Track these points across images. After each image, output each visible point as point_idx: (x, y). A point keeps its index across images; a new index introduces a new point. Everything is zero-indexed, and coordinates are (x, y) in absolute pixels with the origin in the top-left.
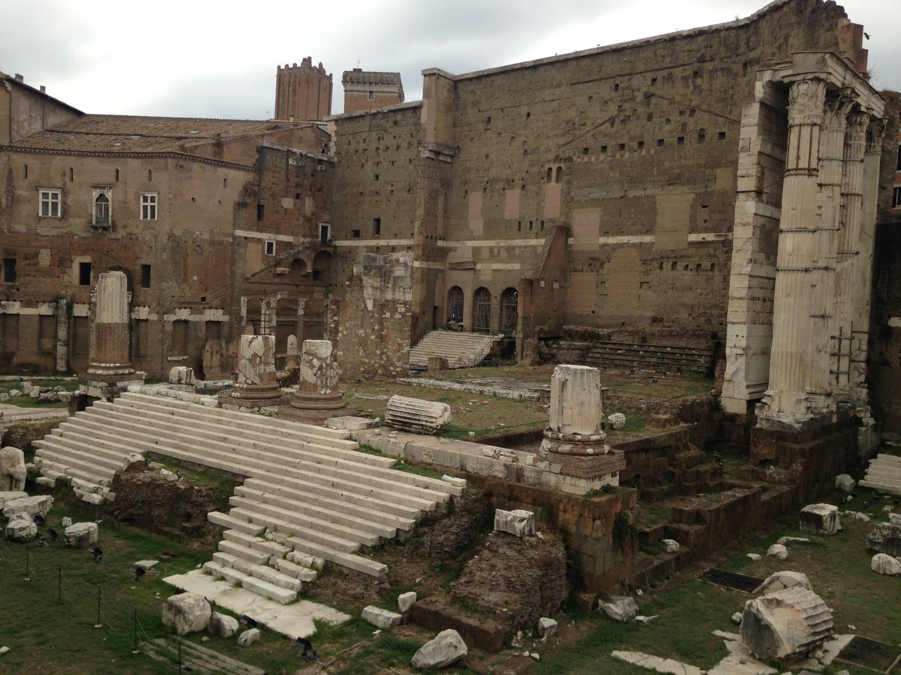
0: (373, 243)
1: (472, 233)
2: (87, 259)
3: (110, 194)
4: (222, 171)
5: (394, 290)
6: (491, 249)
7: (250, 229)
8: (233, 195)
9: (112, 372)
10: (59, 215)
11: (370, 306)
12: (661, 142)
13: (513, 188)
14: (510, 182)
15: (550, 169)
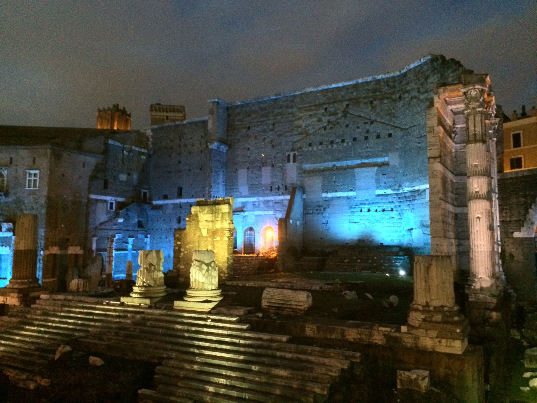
1: (241, 193)
3: (6, 172)
4: (82, 158)
5: (222, 221)
6: (254, 202)
7: (101, 195)
8: (88, 171)
9: (26, 286)
12: (355, 139)
13: (266, 166)
14: (264, 164)
15: (289, 155)
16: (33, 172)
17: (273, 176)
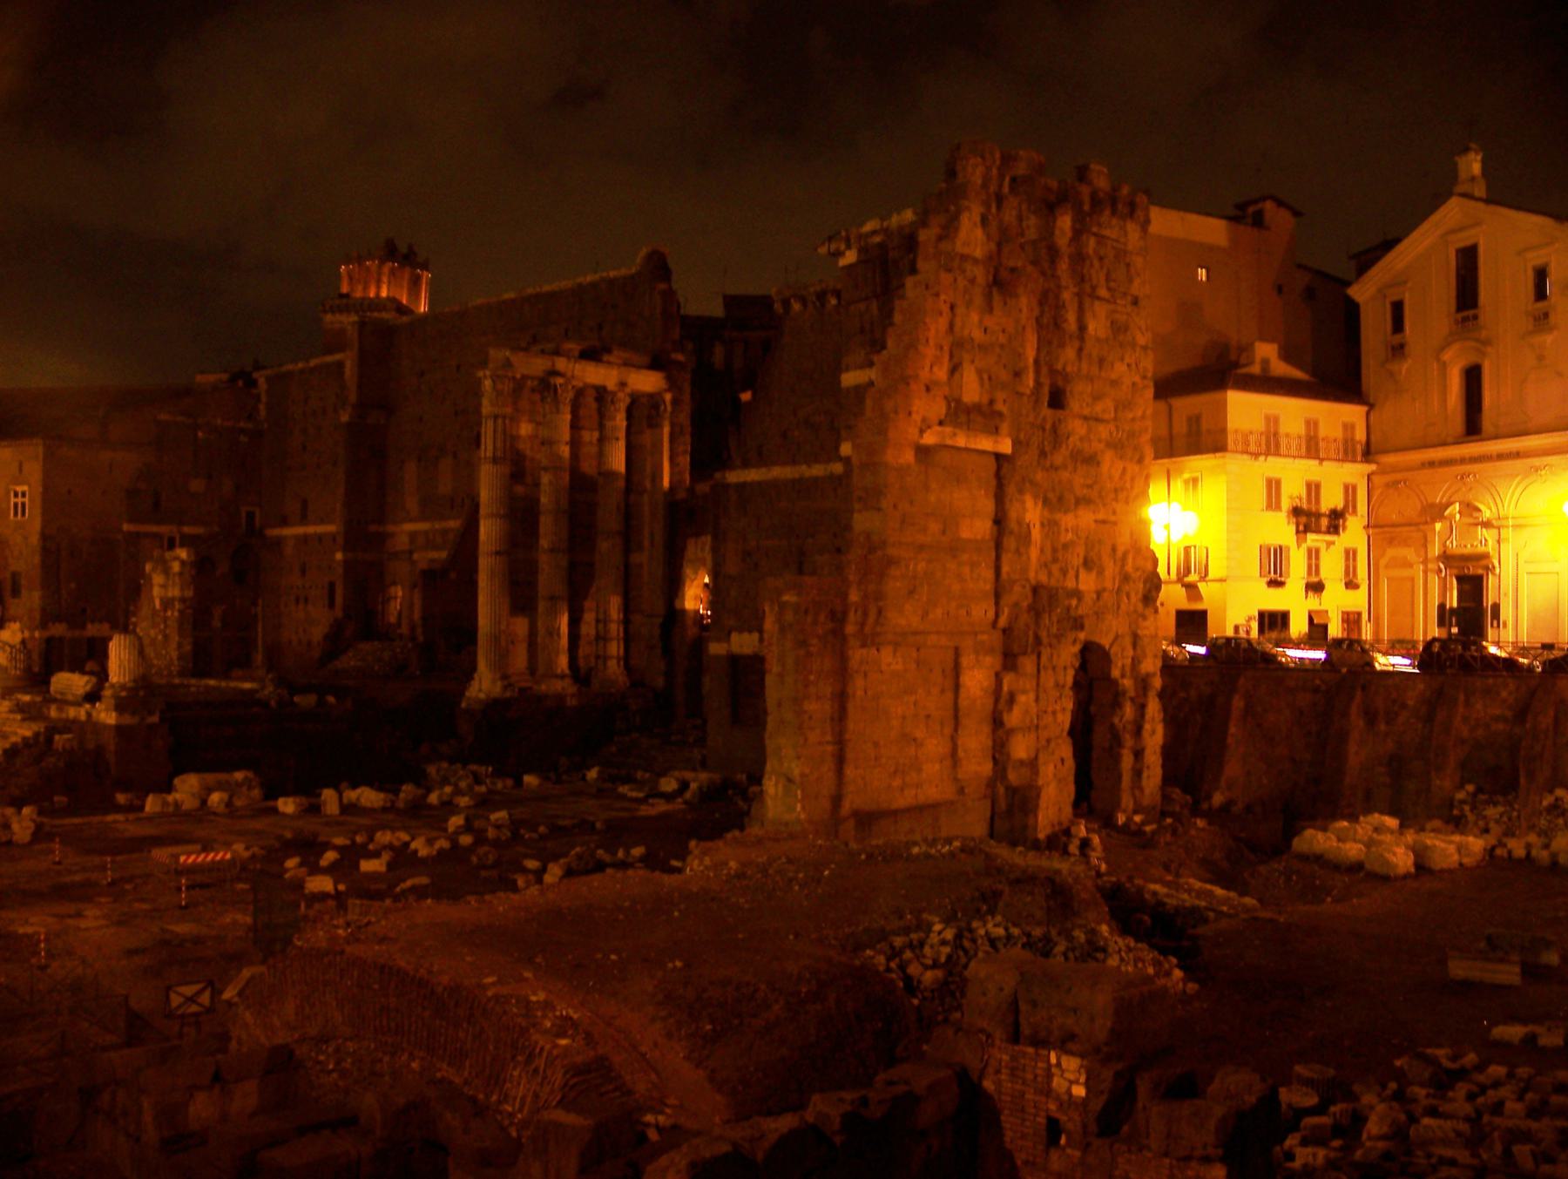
0: (300, 530)
6: (426, 533)
16: (19, 489)
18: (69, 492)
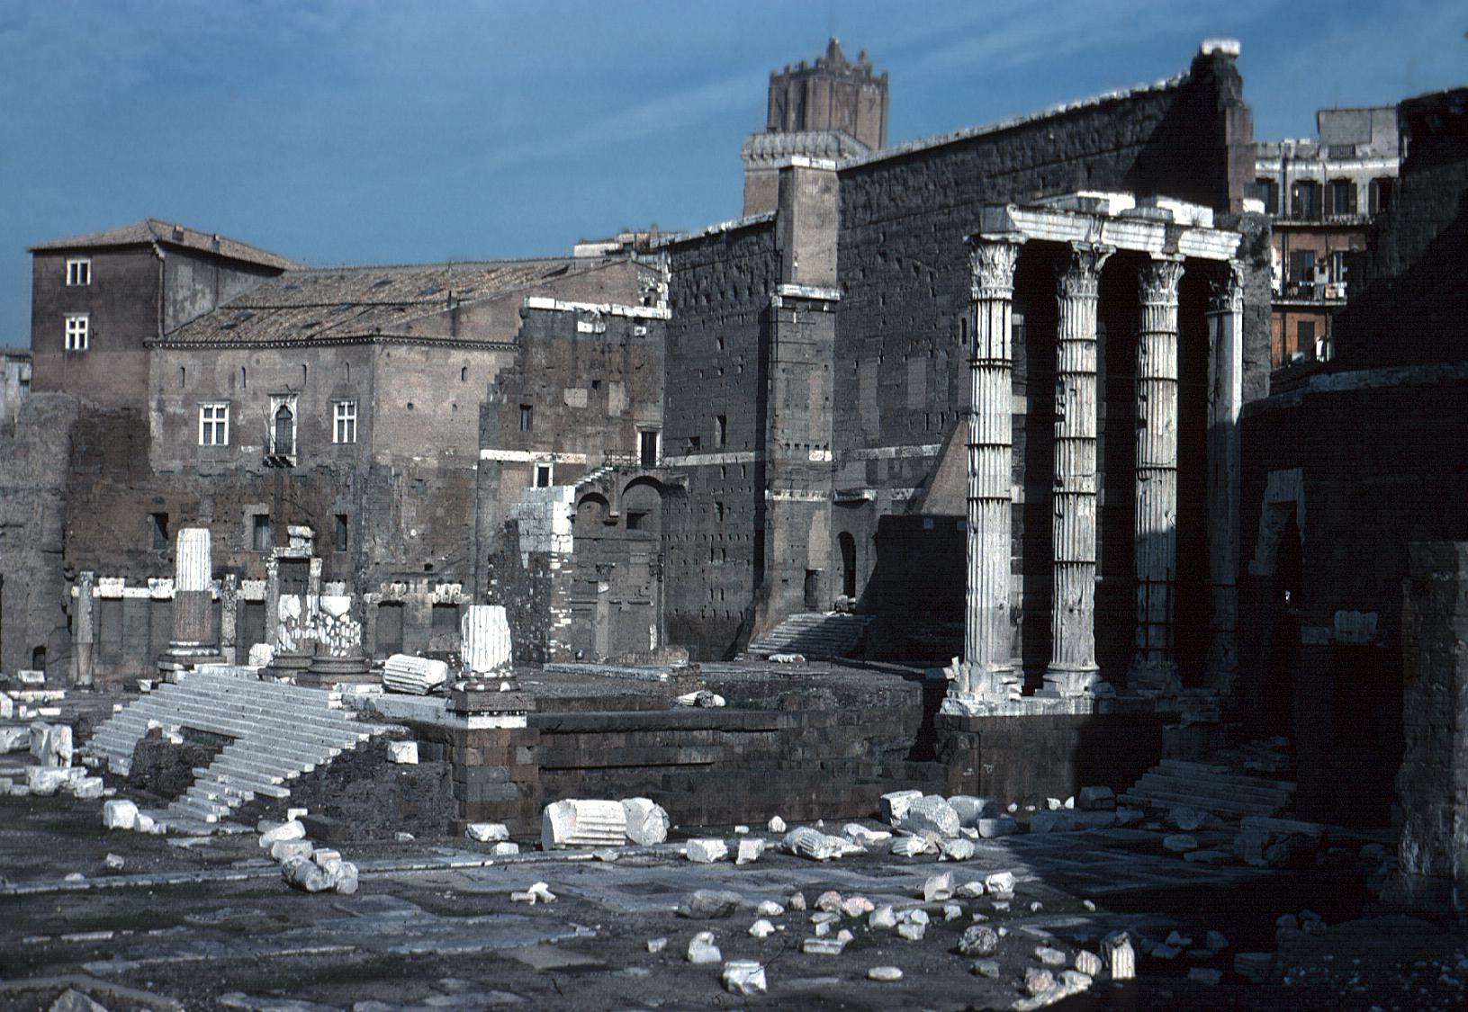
0: (718, 459)
2: (264, 509)
4: (458, 357)
8: (477, 391)
9: (189, 653)
10: (226, 442)
11: (526, 564)
17: (931, 383)
18: (410, 405)
